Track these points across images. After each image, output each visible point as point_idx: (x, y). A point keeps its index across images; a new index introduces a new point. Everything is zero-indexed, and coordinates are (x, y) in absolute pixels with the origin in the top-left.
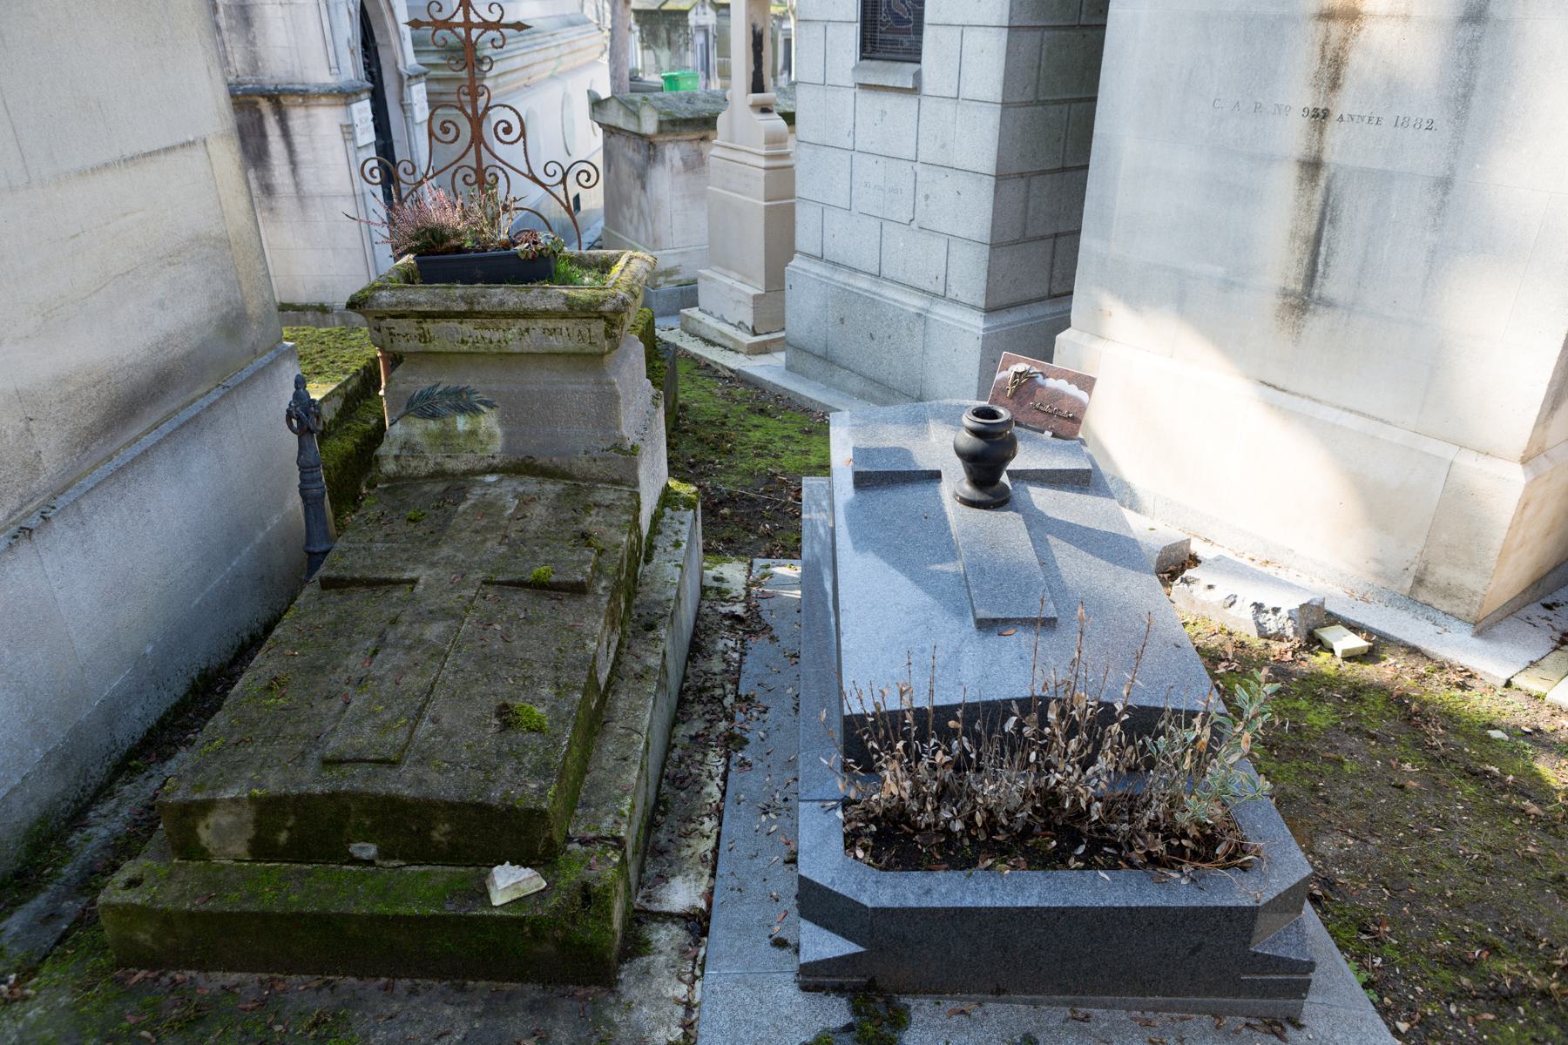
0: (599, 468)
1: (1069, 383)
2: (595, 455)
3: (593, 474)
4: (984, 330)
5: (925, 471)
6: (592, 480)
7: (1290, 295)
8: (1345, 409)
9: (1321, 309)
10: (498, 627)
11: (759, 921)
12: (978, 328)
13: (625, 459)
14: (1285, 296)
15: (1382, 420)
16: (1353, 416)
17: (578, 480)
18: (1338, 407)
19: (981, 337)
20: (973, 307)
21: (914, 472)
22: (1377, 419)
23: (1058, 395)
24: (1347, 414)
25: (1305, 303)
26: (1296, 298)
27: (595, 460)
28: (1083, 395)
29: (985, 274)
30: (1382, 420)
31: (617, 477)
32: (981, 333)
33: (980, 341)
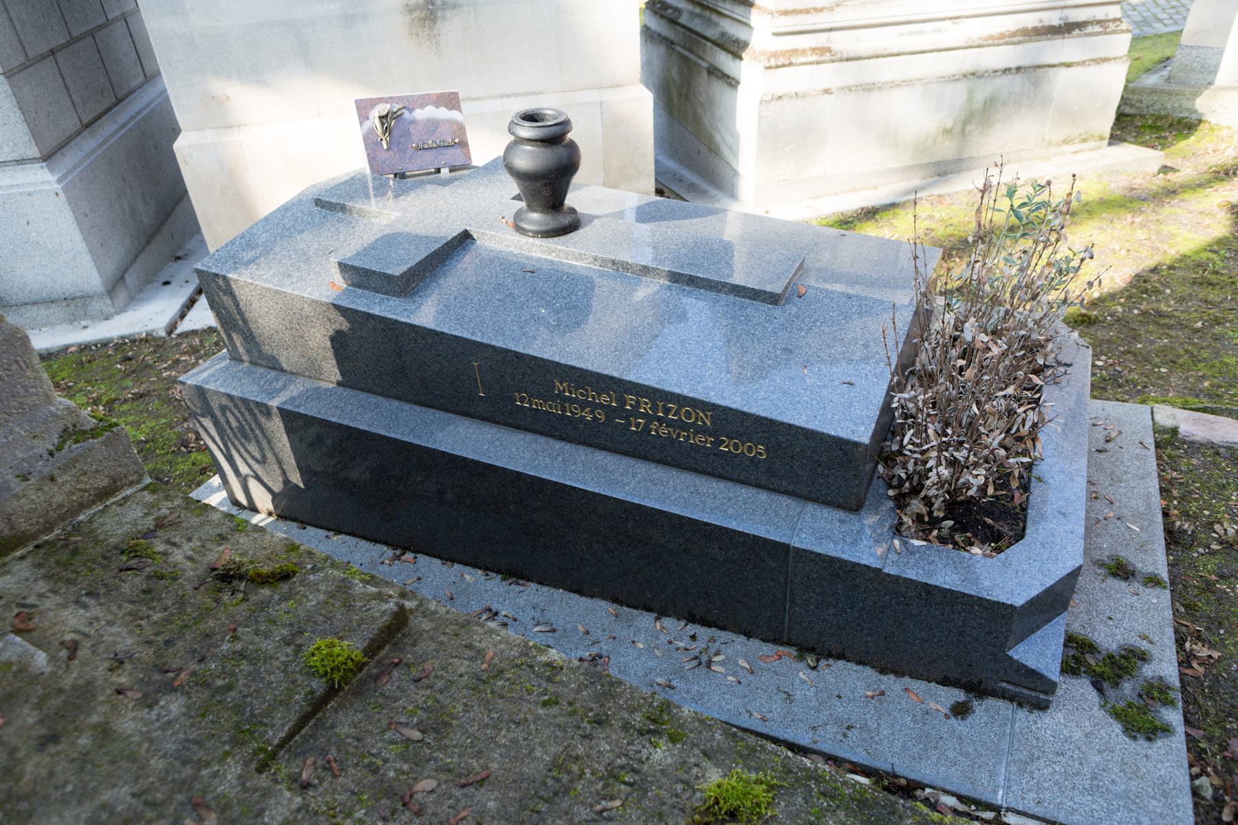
0: (67, 488)
1: (437, 107)
2: (47, 471)
3: (60, 506)
4: (59, 181)
5: (455, 238)
6: (62, 518)
7: (416, 10)
8: (502, 96)
9: (448, 13)
10: (427, 784)
11: (915, 721)
12: (49, 182)
13: (103, 443)
14: (411, 11)
15: (535, 93)
16: (512, 99)
17: (34, 536)
18: (496, 97)
19: (60, 191)
20: (21, 162)
21: (447, 244)
22: (531, 94)
23: (433, 125)
24: (505, 100)
25: (432, 12)
26: (422, 10)
27: (52, 479)
28: (454, 115)
29: (19, 113)
30: (535, 93)
31: (103, 482)
32: (56, 186)
33: (62, 196)
